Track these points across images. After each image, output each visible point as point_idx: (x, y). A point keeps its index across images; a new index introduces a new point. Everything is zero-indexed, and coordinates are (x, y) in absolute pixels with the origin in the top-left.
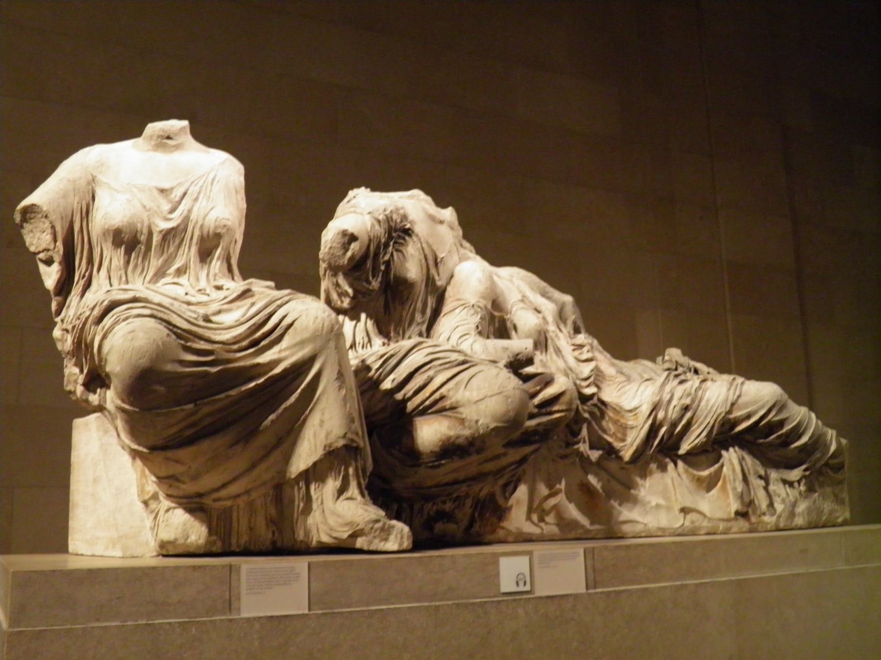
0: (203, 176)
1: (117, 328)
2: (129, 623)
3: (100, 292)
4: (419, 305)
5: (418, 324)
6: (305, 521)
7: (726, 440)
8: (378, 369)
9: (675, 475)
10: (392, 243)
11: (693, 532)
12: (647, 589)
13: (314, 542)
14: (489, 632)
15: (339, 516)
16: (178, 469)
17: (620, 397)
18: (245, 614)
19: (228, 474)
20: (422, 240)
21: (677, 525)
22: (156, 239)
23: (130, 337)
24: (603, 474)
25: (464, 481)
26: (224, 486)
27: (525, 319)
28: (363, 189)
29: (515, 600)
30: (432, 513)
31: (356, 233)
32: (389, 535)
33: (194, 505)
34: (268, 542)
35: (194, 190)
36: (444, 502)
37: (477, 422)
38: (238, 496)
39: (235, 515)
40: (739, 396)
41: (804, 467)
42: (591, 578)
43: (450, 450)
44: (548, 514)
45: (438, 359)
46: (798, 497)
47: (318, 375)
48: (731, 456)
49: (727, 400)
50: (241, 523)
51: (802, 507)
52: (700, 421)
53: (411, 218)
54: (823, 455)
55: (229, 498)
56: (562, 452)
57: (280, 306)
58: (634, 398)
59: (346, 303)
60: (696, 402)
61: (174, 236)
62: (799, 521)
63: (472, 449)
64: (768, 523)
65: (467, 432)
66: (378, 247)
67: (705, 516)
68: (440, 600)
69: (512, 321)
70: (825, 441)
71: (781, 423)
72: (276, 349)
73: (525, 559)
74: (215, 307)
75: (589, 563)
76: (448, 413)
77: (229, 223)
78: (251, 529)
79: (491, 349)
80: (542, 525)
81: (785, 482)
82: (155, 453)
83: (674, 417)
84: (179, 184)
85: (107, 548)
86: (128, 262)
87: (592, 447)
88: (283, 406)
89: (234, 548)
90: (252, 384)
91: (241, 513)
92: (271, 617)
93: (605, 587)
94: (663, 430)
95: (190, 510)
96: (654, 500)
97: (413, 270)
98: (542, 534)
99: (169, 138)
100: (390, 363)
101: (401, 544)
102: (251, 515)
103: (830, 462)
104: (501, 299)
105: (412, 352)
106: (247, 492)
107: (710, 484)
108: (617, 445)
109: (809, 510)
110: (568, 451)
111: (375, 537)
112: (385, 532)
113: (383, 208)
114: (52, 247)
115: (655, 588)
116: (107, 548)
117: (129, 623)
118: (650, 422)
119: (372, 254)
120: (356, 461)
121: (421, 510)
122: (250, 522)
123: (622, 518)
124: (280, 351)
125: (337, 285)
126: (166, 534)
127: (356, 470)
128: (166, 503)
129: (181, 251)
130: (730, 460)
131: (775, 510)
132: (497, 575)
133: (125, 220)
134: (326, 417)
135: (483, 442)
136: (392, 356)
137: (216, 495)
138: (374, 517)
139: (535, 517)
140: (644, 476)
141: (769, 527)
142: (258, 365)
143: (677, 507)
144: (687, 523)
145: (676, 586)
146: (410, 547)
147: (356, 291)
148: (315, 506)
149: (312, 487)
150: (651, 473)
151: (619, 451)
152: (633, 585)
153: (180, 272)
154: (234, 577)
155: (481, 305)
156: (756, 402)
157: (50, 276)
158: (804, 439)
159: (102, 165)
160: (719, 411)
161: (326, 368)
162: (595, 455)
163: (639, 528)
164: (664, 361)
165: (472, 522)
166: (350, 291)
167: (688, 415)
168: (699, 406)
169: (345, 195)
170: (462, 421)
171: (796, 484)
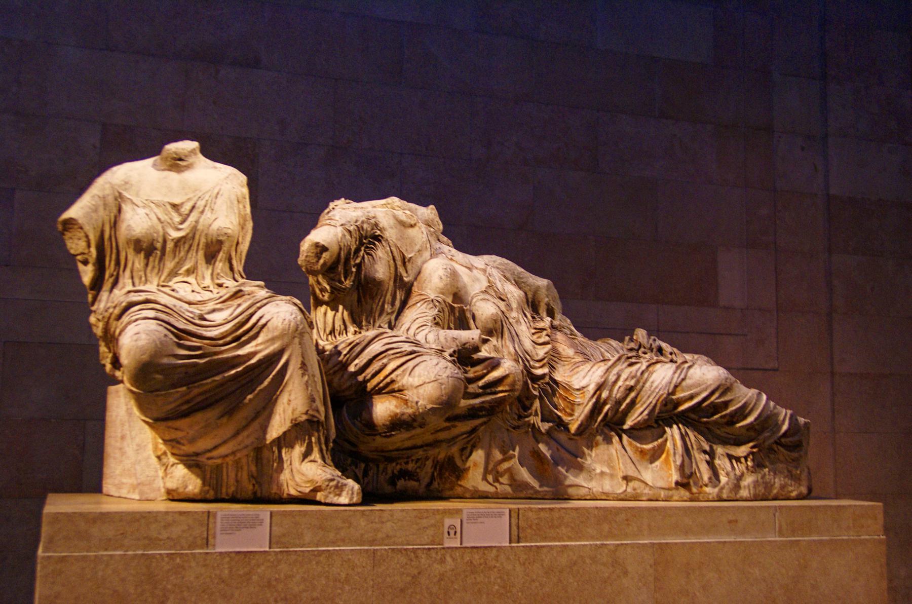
1: (130, 327)
2: (130, 553)
3: (120, 295)
4: (389, 297)
5: (388, 314)
6: (278, 477)
7: (671, 418)
8: (345, 355)
9: (619, 447)
10: (363, 248)
13: (285, 495)
14: (419, 573)
15: (303, 475)
16: (179, 434)
17: (571, 376)
18: (219, 550)
19: (220, 440)
21: (621, 491)
22: (170, 245)
23: (135, 337)
24: (553, 443)
25: (421, 446)
26: (216, 447)
27: (485, 309)
31: (326, 245)
32: (342, 491)
33: (192, 462)
34: (250, 493)
35: (201, 204)
36: (407, 463)
37: (417, 403)
38: (227, 456)
39: (225, 470)
40: (683, 380)
41: (751, 444)
42: (515, 532)
43: (397, 424)
45: (393, 349)
46: (745, 471)
48: (674, 433)
50: (230, 477)
51: (749, 480)
52: (644, 400)
53: (381, 225)
54: (774, 433)
55: (220, 457)
56: (515, 423)
57: (259, 308)
58: (584, 377)
59: (326, 297)
60: (641, 384)
61: (185, 243)
62: (744, 493)
63: (415, 424)
65: (410, 411)
66: (349, 253)
67: (647, 484)
68: (379, 545)
69: (470, 311)
70: (777, 421)
71: (726, 404)
72: (254, 343)
74: (211, 306)
75: (514, 521)
76: (397, 394)
77: (229, 231)
78: (237, 481)
79: (442, 339)
80: (496, 484)
81: (730, 457)
82: (159, 423)
83: (618, 396)
84: (189, 199)
85: (129, 492)
86: (147, 265)
87: (542, 421)
88: (259, 388)
89: (224, 496)
90: (233, 372)
91: (230, 467)
92: (239, 552)
94: (607, 407)
95: (189, 467)
97: (381, 270)
98: (497, 493)
99: (180, 160)
100: (356, 349)
101: (351, 499)
102: (237, 471)
103: (783, 440)
104: (463, 292)
105: (376, 340)
106: (234, 453)
107: (654, 456)
108: (566, 419)
109: (756, 484)
112: (339, 488)
113: (355, 219)
114: (86, 251)
115: (575, 546)
116: (129, 492)
117: (130, 553)
118: (594, 400)
119: (342, 260)
120: (318, 431)
121: (385, 469)
122: (236, 475)
123: (567, 482)
124: (257, 345)
125: (319, 283)
126: (171, 484)
127: (319, 439)
128: (172, 460)
129: (190, 255)
130: (672, 436)
131: (719, 481)
133: (144, 231)
134: (292, 397)
135: (423, 418)
136: (358, 344)
138: (329, 476)
139: (490, 478)
140: (590, 447)
141: (710, 497)
142: (239, 356)
143: (621, 474)
145: (596, 545)
146: (360, 501)
147: (331, 287)
148: (285, 466)
149: (284, 451)
150: (597, 444)
151: (568, 424)
153: (189, 272)
154: (211, 520)
156: (699, 385)
157: (87, 274)
158: (750, 419)
159: (126, 183)
160: (661, 392)
161: (292, 358)
162: (544, 427)
163: (582, 492)
164: (631, 340)
165: (432, 478)
166: (328, 287)
167: (633, 395)
169: (327, 206)
170: (406, 402)
171: (743, 460)
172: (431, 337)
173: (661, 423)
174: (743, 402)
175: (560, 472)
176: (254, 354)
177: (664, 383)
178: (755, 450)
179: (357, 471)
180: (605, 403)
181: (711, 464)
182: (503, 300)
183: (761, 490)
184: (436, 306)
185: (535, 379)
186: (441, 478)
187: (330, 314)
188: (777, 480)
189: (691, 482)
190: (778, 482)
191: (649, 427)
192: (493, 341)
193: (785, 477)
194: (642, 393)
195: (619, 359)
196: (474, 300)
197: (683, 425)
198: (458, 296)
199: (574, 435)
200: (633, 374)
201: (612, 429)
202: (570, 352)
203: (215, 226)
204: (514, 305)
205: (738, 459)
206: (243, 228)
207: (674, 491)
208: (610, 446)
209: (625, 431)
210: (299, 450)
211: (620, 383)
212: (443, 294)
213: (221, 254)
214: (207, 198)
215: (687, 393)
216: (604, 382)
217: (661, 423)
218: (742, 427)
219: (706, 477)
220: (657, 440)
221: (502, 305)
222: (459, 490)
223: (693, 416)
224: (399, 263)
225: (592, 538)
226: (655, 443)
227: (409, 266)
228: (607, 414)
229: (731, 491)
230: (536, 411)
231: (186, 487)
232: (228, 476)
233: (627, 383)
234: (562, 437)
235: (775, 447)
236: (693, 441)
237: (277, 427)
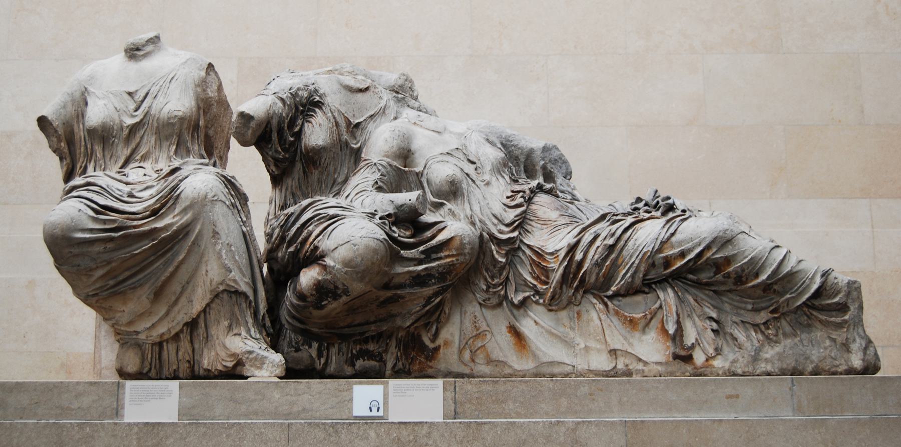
12: (514, 422)
18: (127, 420)
29: (366, 423)
31: (252, 114)
35: (154, 90)
40: (673, 234)
48: (668, 297)
53: (321, 91)
60: (622, 243)
71: (728, 260)
75: (450, 395)
83: (596, 257)
92: (147, 423)
93: (466, 418)
99: (138, 49)
109: (781, 356)
112: (260, 362)
115: (524, 423)
132: (351, 400)
135: (344, 285)
136: (292, 214)
153: (144, 158)
154: (121, 391)
155: (383, 163)
158: (763, 277)
159: (92, 78)
160: (645, 250)
163: (569, 369)
165: (397, 359)
167: (613, 256)
168: (624, 246)
170: (325, 267)
172: (368, 201)
173: (653, 286)
174: (750, 257)
180: (581, 264)
183: (790, 363)
185: (500, 243)
186: (407, 359)
191: (637, 292)
192: (449, 205)
193: (825, 348)
194: (624, 253)
195: (603, 217)
200: (612, 232)
202: (554, 215)
203: (166, 110)
211: (598, 243)
212: (387, 157)
215: (677, 250)
216: (578, 242)
217: (653, 286)
218: (753, 286)
221: (469, 169)
222: (430, 371)
225: (547, 414)
233: (605, 242)
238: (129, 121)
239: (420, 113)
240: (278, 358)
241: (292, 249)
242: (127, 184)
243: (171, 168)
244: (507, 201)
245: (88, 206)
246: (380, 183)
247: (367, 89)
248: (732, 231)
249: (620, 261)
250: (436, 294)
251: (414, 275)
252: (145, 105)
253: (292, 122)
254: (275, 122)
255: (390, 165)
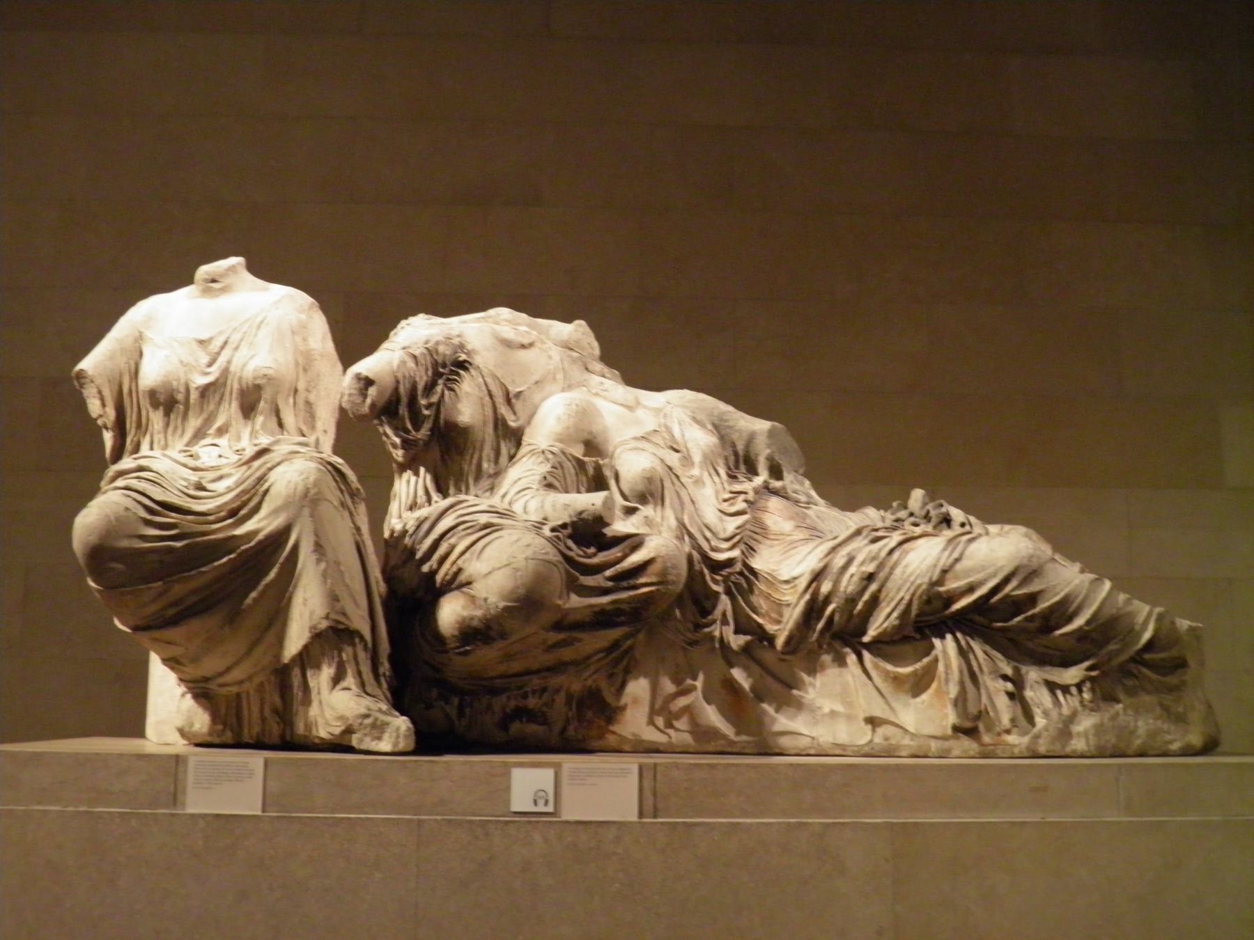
0: (247, 320)
2: (70, 809)
4: (488, 451)
6: (306, 713)
11: (890, 752)
12: (738, 823)
17: (780, 562)
18: (191, 810)
20: (485, 371)
22: (194, 396)
24: (756, 668)
25: (538, 672)
27: (632, 464)
28: (422, 316)
29: (530, 822)
30: (508, 710)
31: (371, 376)
32: (383, 732)
35: (235, 338)
36: (525, 696)
37: (486, 600)
40: (957, 560)
41: (1086, 664)
42: (649, 801)
43: (473, 634)
44: (678, 716)
46: (1080, 708)
47: (296, 548)
48: (946, 647)
49: (935, 566)
50: (252, 712)
51: (1086, 723)
60: (887, 570)
62: (1078, 745)
64: (1015, 746)
65: (479, 613)
67: (906, 731)
69: (613, 467)
71: (1033, 599)
73: (549, 774)
75: (647, 784)
77: (270, 372)
80: (671, 731)
81: (1052, 686)
83: (850, 589)
84: (220, 333)
86: (167, 425)
87: (737, 632)
89: (246, 738)
90: (225, 560)
92: (218, 816)
96: (827, 706)
99: (214, 281)
101: (395, 744)
104: (599, 440)
106: (250, 678)
107: (918, 685)
108: (770, 628)
109: (1099, 729)
110: (698, 636)
111: (365, 735)
112: (378, 729)
113: (424, 339)
115: (751, 824)
117: (70, 809)
118: (807, 597)
119: (404, 400)
123: (777, 728)
129: (222, 408)
130: (945, 652)
132: (508, 789)
136: (426, 518)
137: (221, 680)
138: (363, 711)
139: (660, 721)
140: (812, 672)
142: (234, 537)
143: (862, 716)
144: (878, 740)
145: (789, 824)
149: (309, 673)
150: (823, 668)
152: (747, 817)
153: (221, 431)
154: (181, 769)
155: (554, 450)
156: (983, 568)
158: (1079, 622)
160: (919, 582)
163: (803, 743)
165: (567, 721)
167: (873, 587)
168: (890, 574)
170: (473, 598)
172: (533, 505)
173: (927, 632)
174: (1062, 594)
175: (764, 712)
176: (255, 532)
177: (924, 567)
178: (1094, 673)
179: (448, 708)
180: (827, 600)
181: (1016, 696)
182: (677, 451)
183: (1111, 739)
184: (548, 460)
185: (716, 567)
186: (579, 721)
187: (413, 479)
188: (1140, 723)
189: (981, 727)
190: (1144, 726)
191: (906, 639)
194: (890, 585)
195: (858, 532)
196: (618, 451)
197: (964, 633)
198: (592, 447)
199: (783, 653)
201: (847, 644)
202: (788, 526)
203: (251, 367)
204: (697, 458)
205: (1066, 689)
206: (305, 370)
207: (952, 743)
208: (844, 670)
209: (867, 646)
210: (327, 672)
212: (561, 441)
213: (262, 404)
214: (245, 329)
217: (927, 632)
219: (1005, 720)
220: (920, 660)
221: (673, 459)
223: (978, 618)
224: (500, 400)
225: (784, 814)
226: (918, 666)
227: (518, 405)
228: (831, 619)
229: (1054, 740)
230: (724, 614)
231: (192, 725)
232: (249, 709)
233: (864, 569)
234: (768, 657)
235: (1132, 666)
236: (981, 660)
237: (295, 640)
238: (202, 381)
239: (603, 379)
240: (402, 723)
241: (425, 568)
242: (195, 469)
243: (257, 449)
244: (726, 507)
245: (139, 502)
246: (549, 478)
247: (531, 345)
248: (1039, 557)
249: (883, 595)
250: (627, 637)
251: (597, 609)
252: (222, 360)
253: (430, 388)
254: (402, 390)
255: (564, 453)
